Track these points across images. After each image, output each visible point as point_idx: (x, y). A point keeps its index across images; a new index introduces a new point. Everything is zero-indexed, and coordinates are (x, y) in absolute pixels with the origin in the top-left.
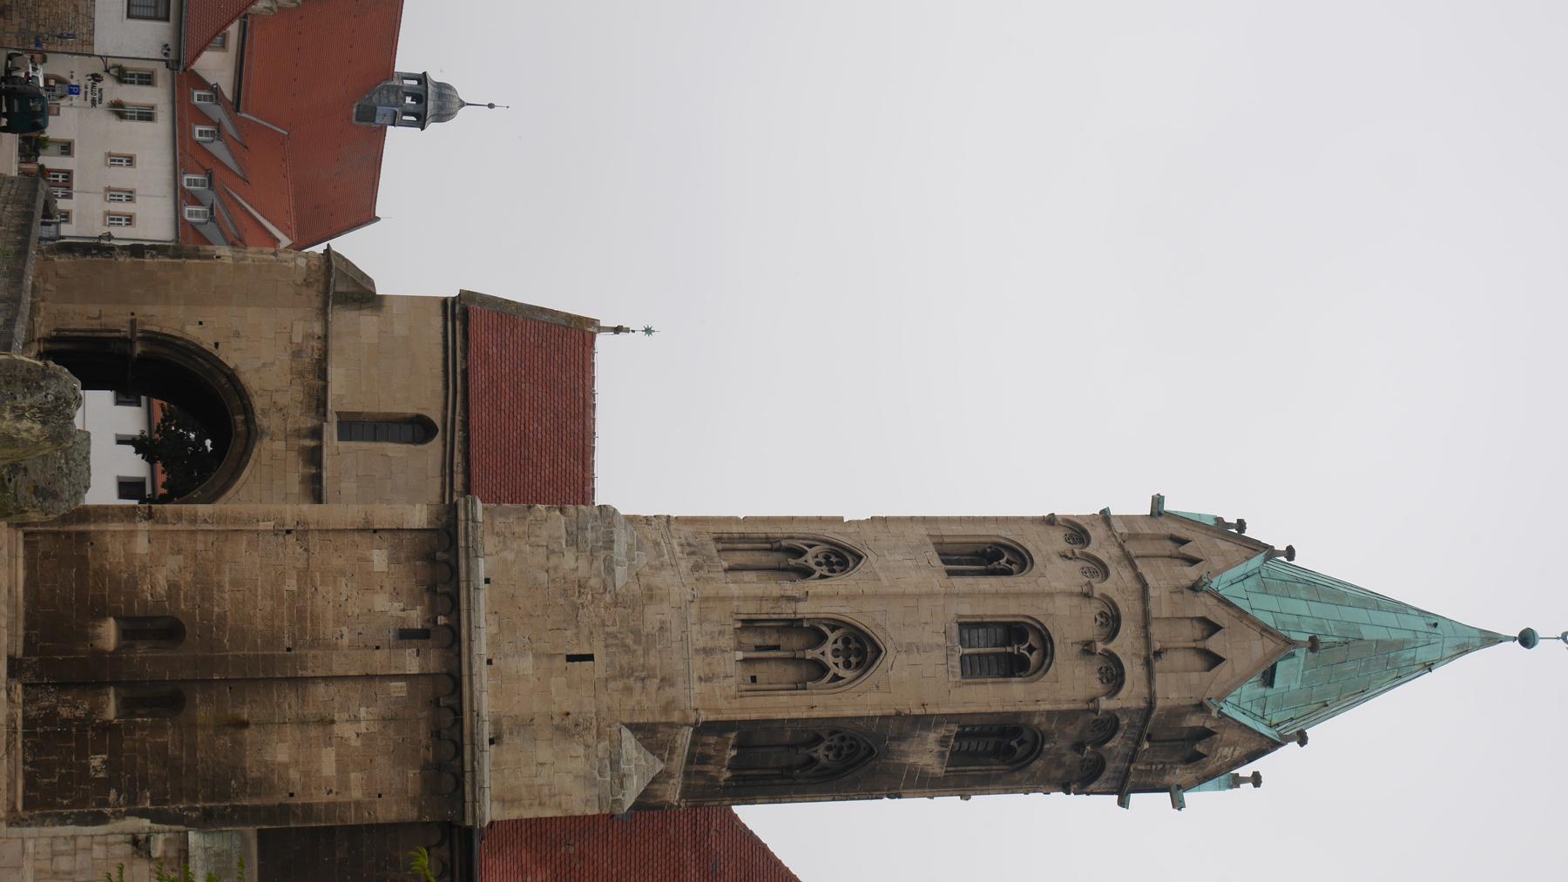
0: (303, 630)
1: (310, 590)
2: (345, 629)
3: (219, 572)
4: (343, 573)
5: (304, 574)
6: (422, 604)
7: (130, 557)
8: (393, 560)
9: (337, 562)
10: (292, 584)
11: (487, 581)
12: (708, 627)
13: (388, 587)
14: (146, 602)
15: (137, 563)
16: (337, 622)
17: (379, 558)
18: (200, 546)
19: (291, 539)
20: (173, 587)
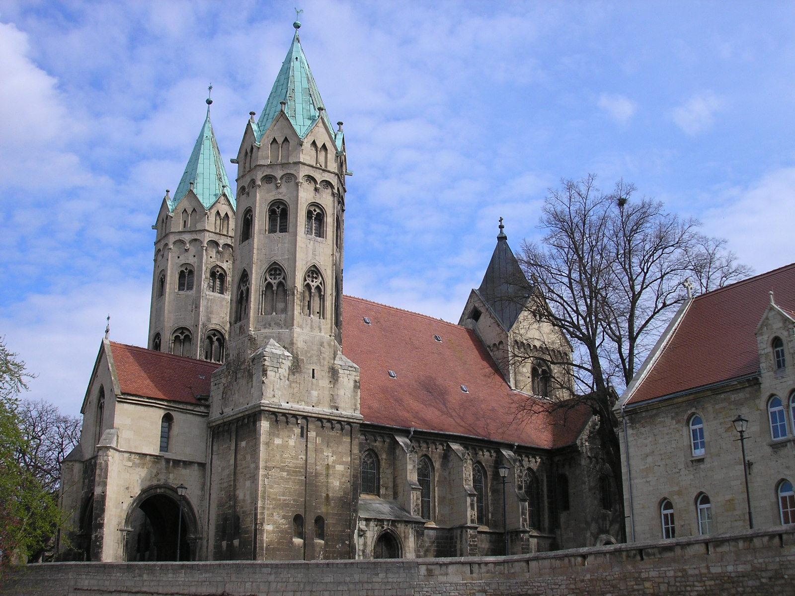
0: (300, 472)
1: (286, 468)
2: (300, 457)
3: (280, 500)
4: (282, 455)
5: (282, 469)
6: (293, 428)
7: (273, 532)
8: (278, 436)
9: (278, 457)
10: (285, 474)
11: (288, 403)
12: (304, 326)
13: (286, 439)
14: (288, 527)
15: (276, 530)
16: (297, 459)
17: (278, 441)
18: (271, 506)
19: (270, 473)
20: (284, 517)
